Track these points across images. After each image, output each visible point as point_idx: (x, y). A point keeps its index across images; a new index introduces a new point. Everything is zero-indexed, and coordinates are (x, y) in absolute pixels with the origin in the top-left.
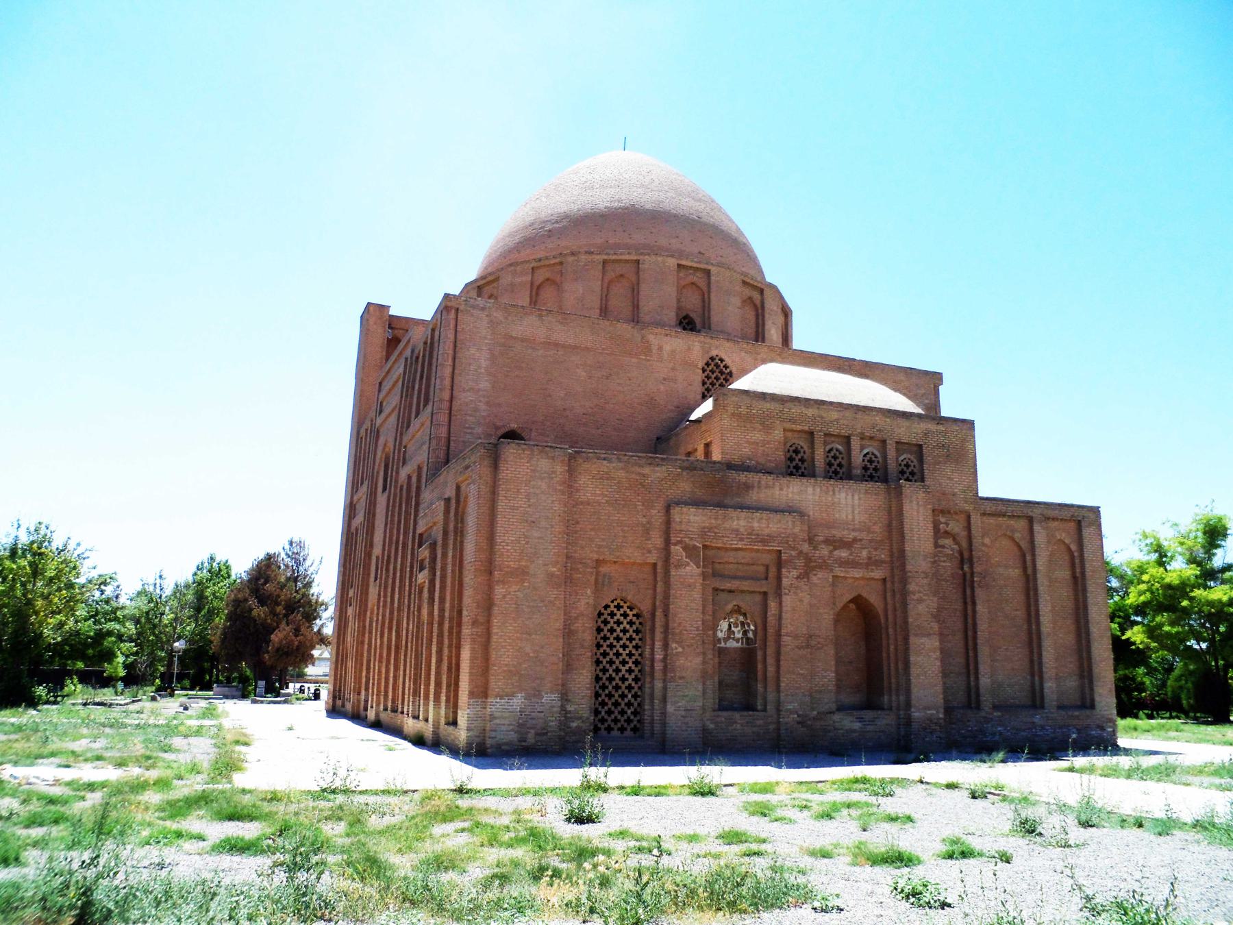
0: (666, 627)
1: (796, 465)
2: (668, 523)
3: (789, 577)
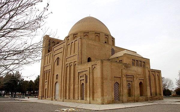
0: (122, 86)
1: (133, 64)
2: (122, 72)
3: (135, 79)
